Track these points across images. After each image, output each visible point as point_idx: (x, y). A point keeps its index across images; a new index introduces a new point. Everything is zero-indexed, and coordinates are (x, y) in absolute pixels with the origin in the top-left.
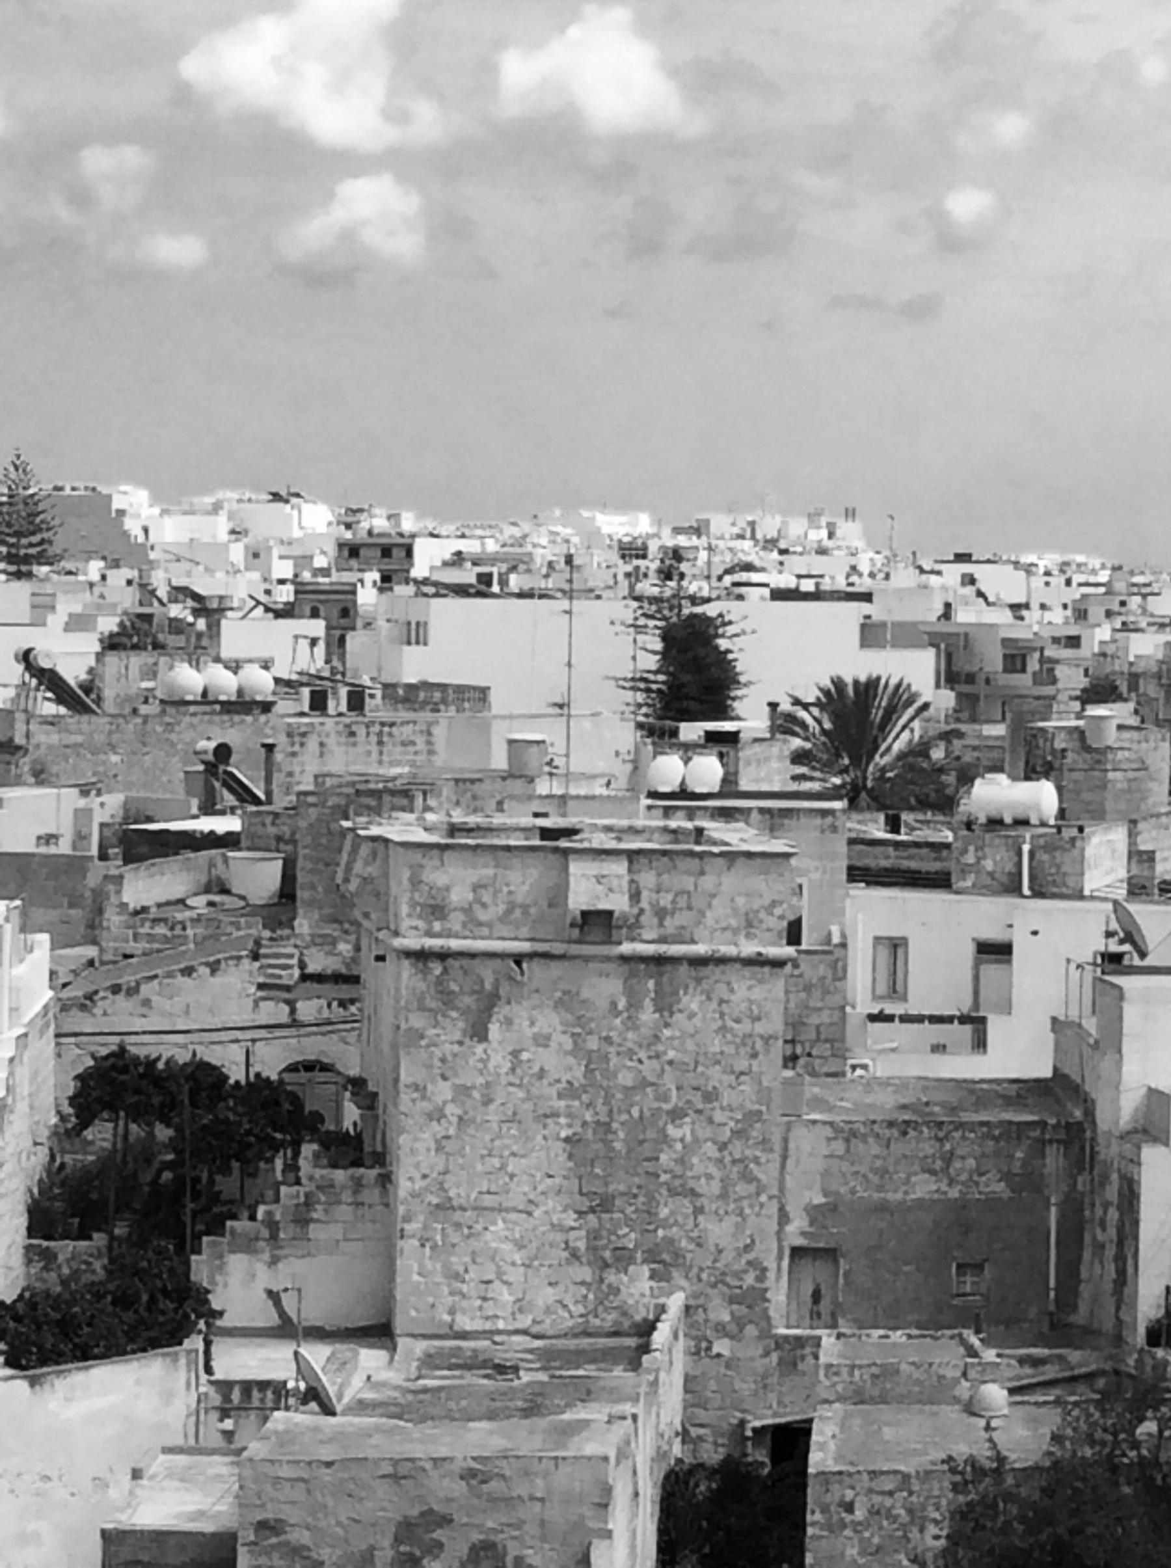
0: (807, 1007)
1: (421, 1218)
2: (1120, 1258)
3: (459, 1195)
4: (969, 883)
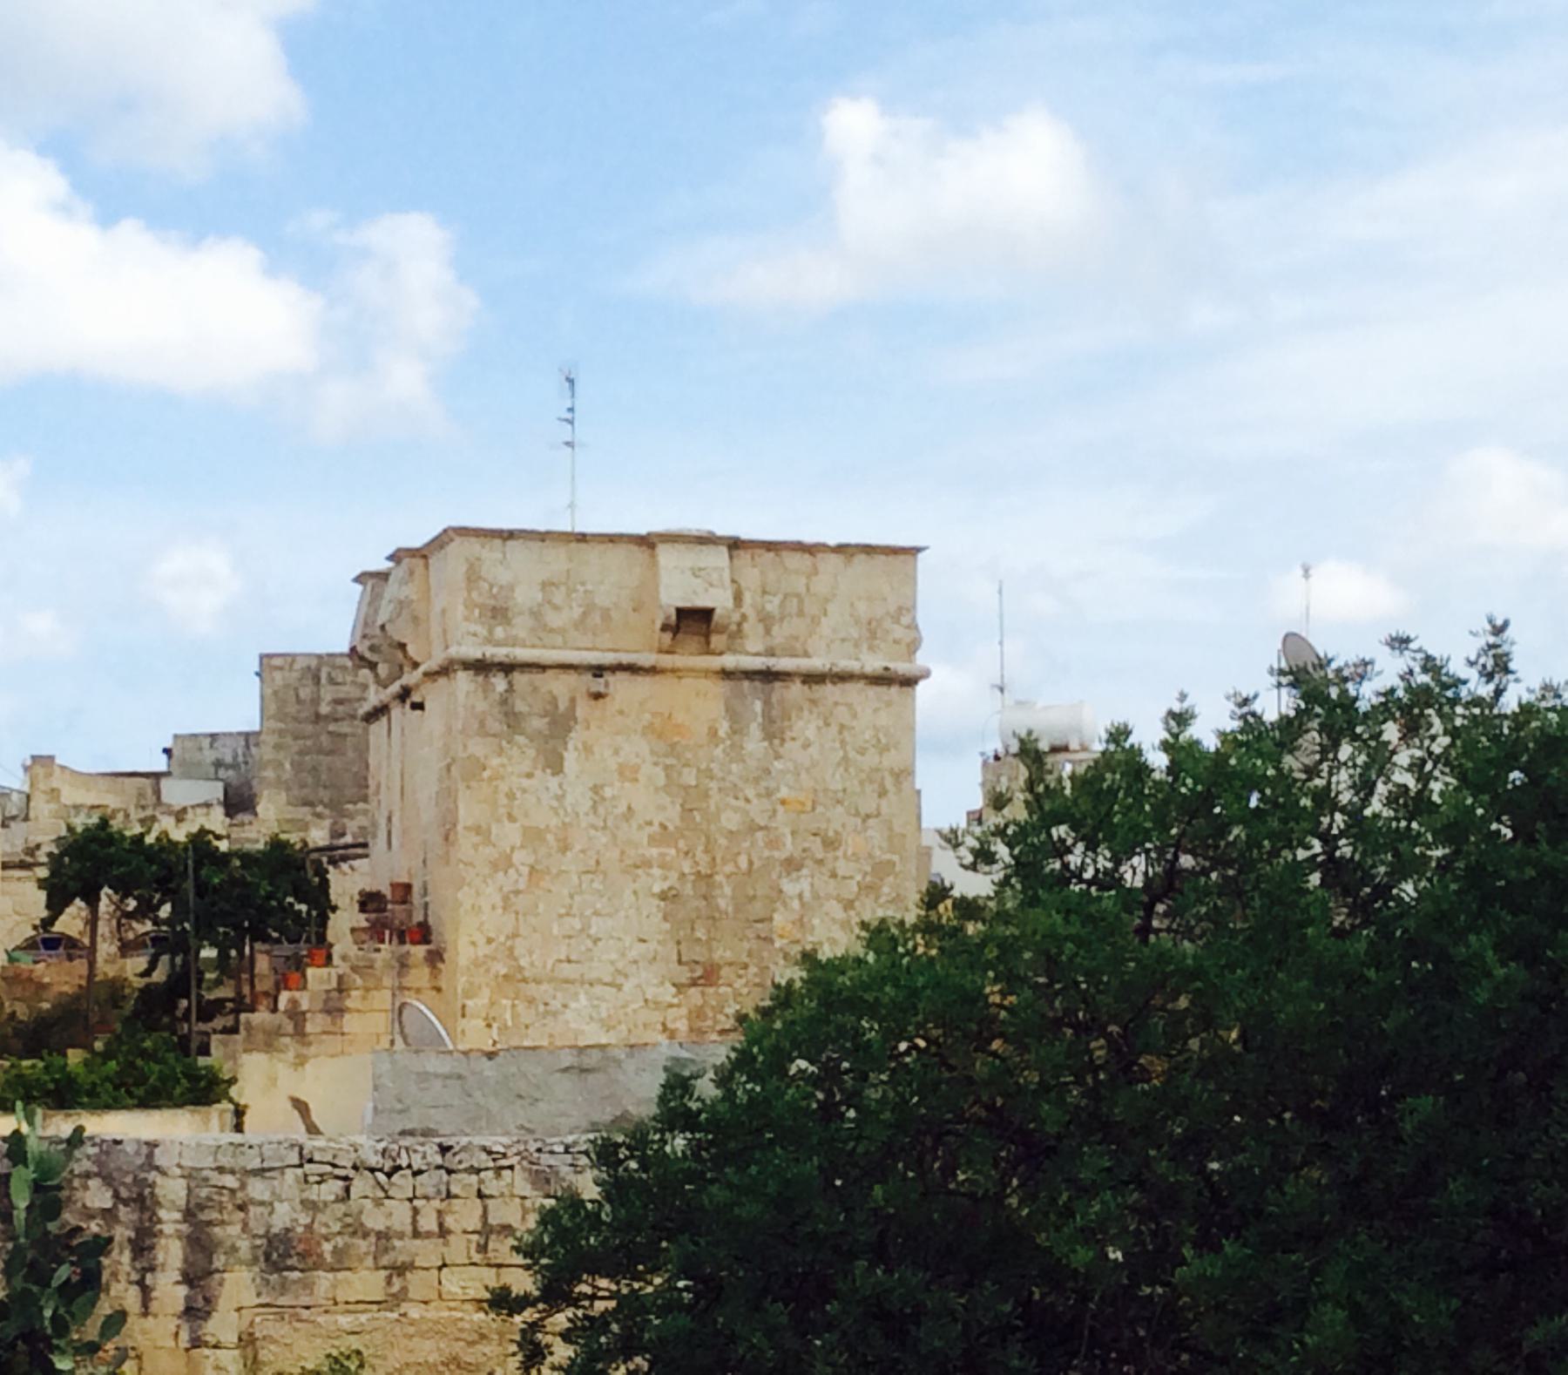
1: (486, 992)
3: (532, 964)
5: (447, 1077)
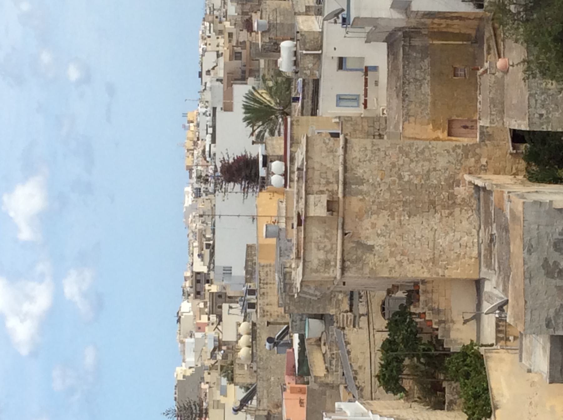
0: (362, 131)
1: (437, 269)
2: (452, 18)
3: (429, 255)
4: (317, 73)
5: (531, 313)
